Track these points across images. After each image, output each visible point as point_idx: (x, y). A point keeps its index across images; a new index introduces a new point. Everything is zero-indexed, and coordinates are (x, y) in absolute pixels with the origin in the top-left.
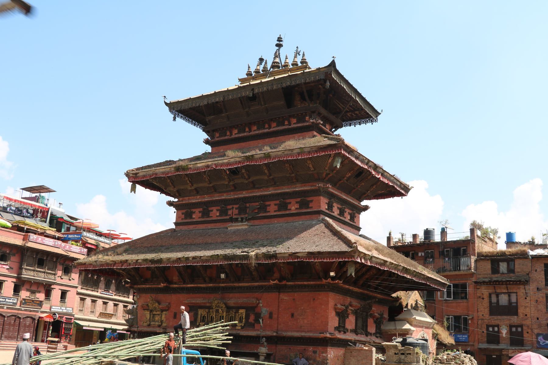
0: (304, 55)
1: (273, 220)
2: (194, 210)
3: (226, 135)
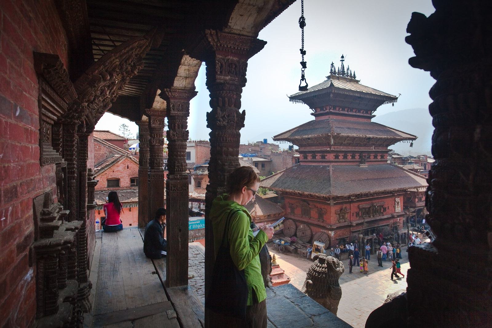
0: (354, 73)
1: (373, 163)
2: (339, 154)
3: (336, 110)
